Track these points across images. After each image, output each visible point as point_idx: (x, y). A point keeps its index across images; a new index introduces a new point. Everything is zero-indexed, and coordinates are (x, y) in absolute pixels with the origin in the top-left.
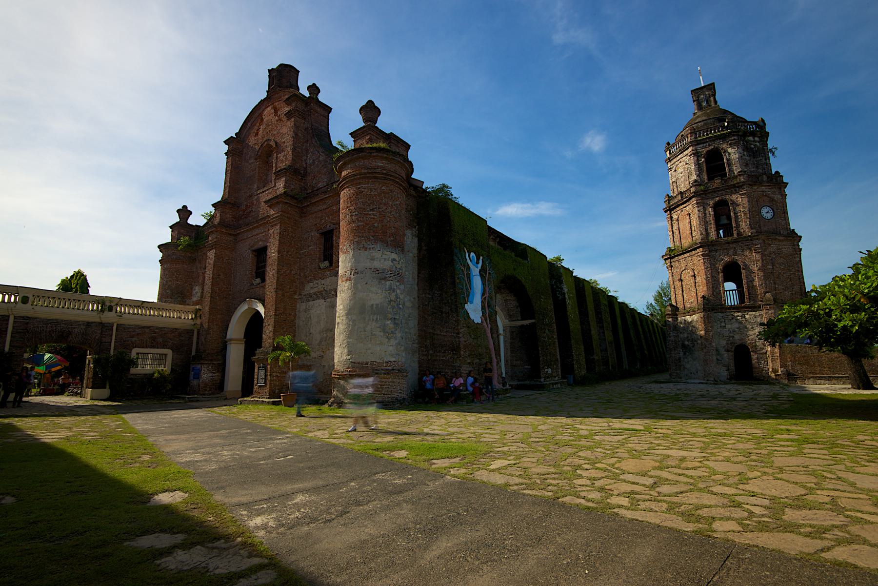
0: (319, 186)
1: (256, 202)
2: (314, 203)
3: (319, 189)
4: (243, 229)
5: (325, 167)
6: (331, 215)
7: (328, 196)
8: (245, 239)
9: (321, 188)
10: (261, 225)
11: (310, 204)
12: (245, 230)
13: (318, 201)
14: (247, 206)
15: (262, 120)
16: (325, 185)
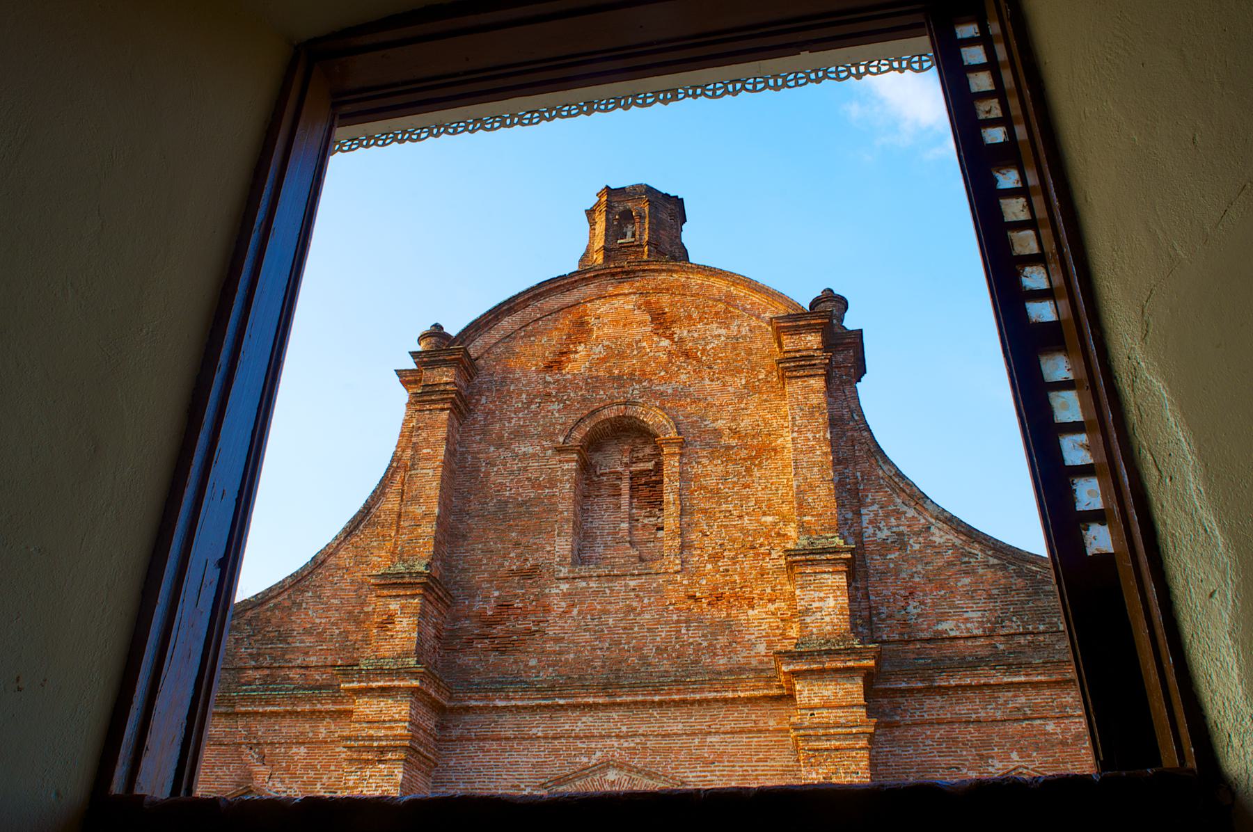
0: (940, 627)
1: (563, 604)
2: (948, 688)
3: (943, 639)
4: (507, 698)
5: (966, 573)
6: (1038, 749)
7: (1023, 679)
8: (507, 739)
9: (955, 638)
10: (620, 704)
11: (928, 689)
12: (519, 703)
13: (970, 686)
14: (504, 606)
15: (581, 329)
16: (979, 632)
